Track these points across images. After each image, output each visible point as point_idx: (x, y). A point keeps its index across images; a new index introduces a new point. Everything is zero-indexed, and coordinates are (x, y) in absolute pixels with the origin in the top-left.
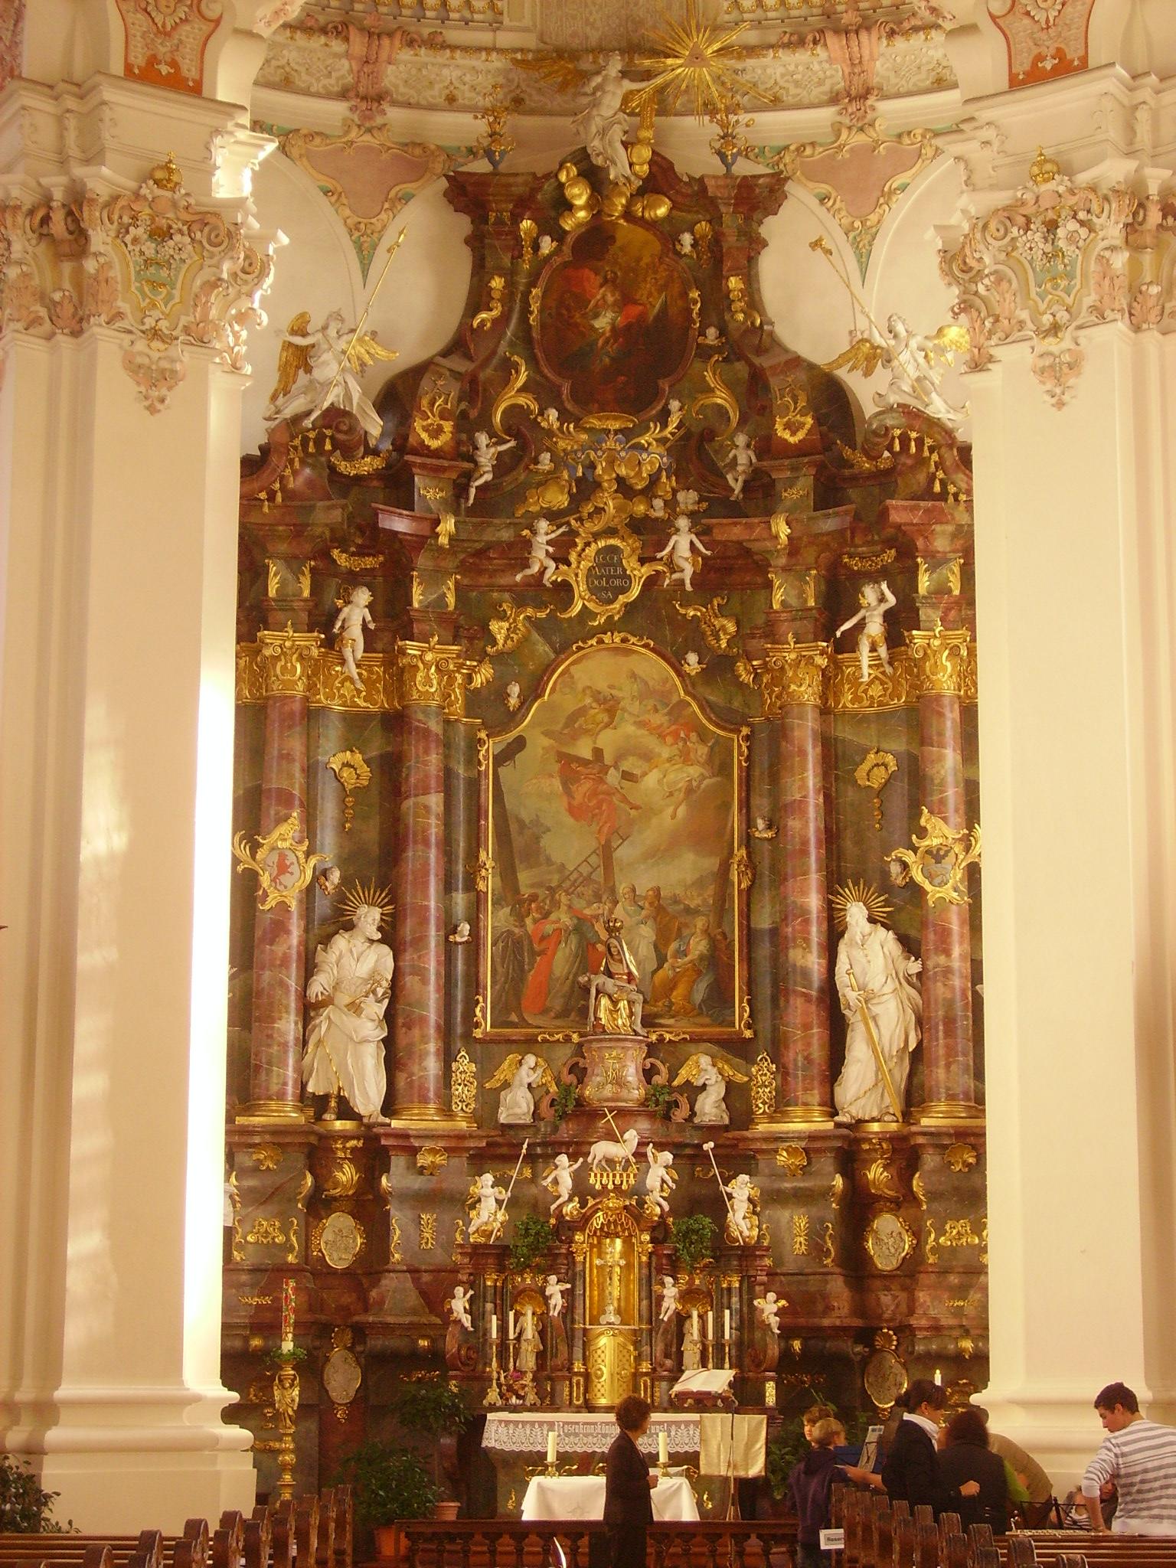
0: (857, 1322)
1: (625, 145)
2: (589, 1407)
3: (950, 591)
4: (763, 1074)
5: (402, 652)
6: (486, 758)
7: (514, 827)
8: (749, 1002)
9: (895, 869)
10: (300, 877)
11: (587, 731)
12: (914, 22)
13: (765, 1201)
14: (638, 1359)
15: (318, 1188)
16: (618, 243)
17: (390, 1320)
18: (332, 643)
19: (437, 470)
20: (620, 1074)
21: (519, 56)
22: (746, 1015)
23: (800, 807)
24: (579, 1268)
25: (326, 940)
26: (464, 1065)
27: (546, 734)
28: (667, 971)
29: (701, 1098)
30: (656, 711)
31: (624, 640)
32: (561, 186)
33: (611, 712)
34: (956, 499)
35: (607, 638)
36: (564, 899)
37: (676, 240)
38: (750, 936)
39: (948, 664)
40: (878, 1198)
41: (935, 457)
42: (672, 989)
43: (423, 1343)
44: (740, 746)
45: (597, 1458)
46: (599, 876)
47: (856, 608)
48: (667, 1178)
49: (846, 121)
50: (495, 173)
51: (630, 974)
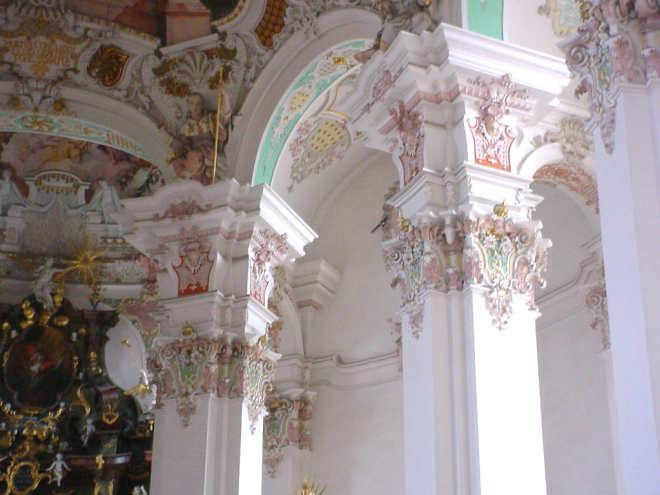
1: (53, 295)
32: (22, 310)
37: (70, 335)
49: (146, 290)
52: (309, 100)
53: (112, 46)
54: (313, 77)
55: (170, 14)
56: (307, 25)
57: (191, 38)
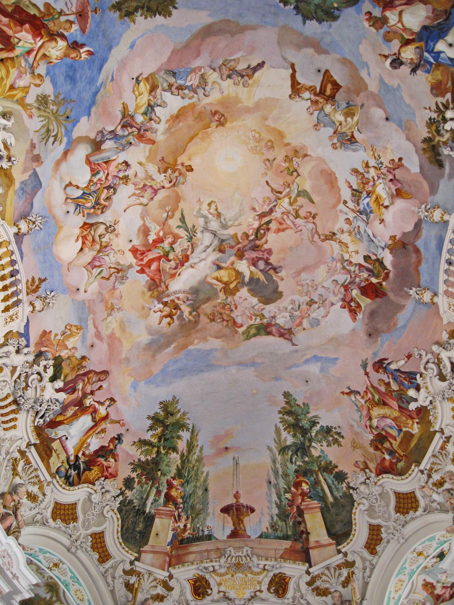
52: (405, 584)
53: (280, 573)
54: (405, 568)
55: (312, 548)
56: (397, 534)
57: (325, 560)
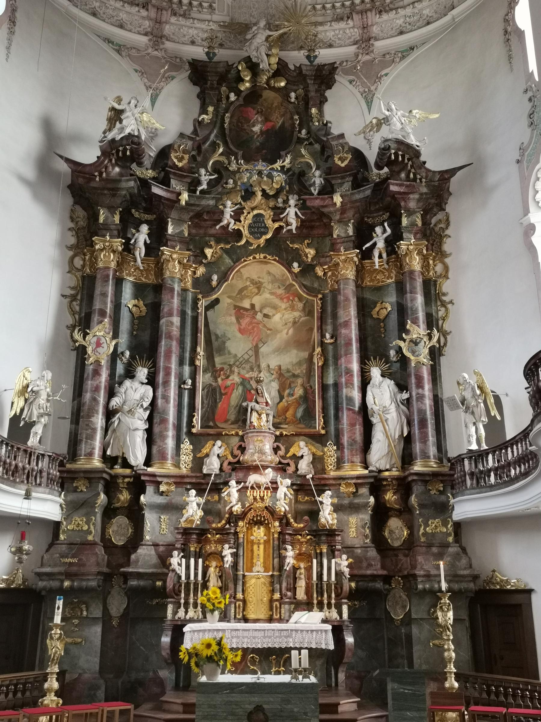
0: (385, 572)
1: (268, 55)
2: (246, 620)
3: (417, 225)
4: (331, 450)
5: (163, 254)
6: (202, 306)
7: (213, 338)
8: (323, 417)
9: (392, 353)
10: (108, 348)
11: (248, 296)
12: (391, 6)
13: (337, 508)
14: (273, 592)
15: (110, 502)
16: (263, 98)
17: (141, 570)
18: (128, 248)
19: (180, 177)
20: (262, 447)
21: (222, 24)
22: (322, 423)
23: (347, 324)
24: (241, 540)
25: (120, 384)
26: (187, 446)
27: (229, 297)
28: (284, 403)
29: (301, 462)
30: (279, 288)
31: (265, 257)
33: (259, 288)
34: (421, 182)
35: (257, 256)
36: (236, 370)
38: (324, 388)
39: (417, 257)
40: (391, 509)
41: (410, 163)
42: (286, 411)
43: (159, 583)
44: (317, 303)
45: (249, 651)
46: (253, 359)
47: (372, 238)
48: (288, 493)
49: (361, 51)
50: (210, 62)
51: (267, 403)
